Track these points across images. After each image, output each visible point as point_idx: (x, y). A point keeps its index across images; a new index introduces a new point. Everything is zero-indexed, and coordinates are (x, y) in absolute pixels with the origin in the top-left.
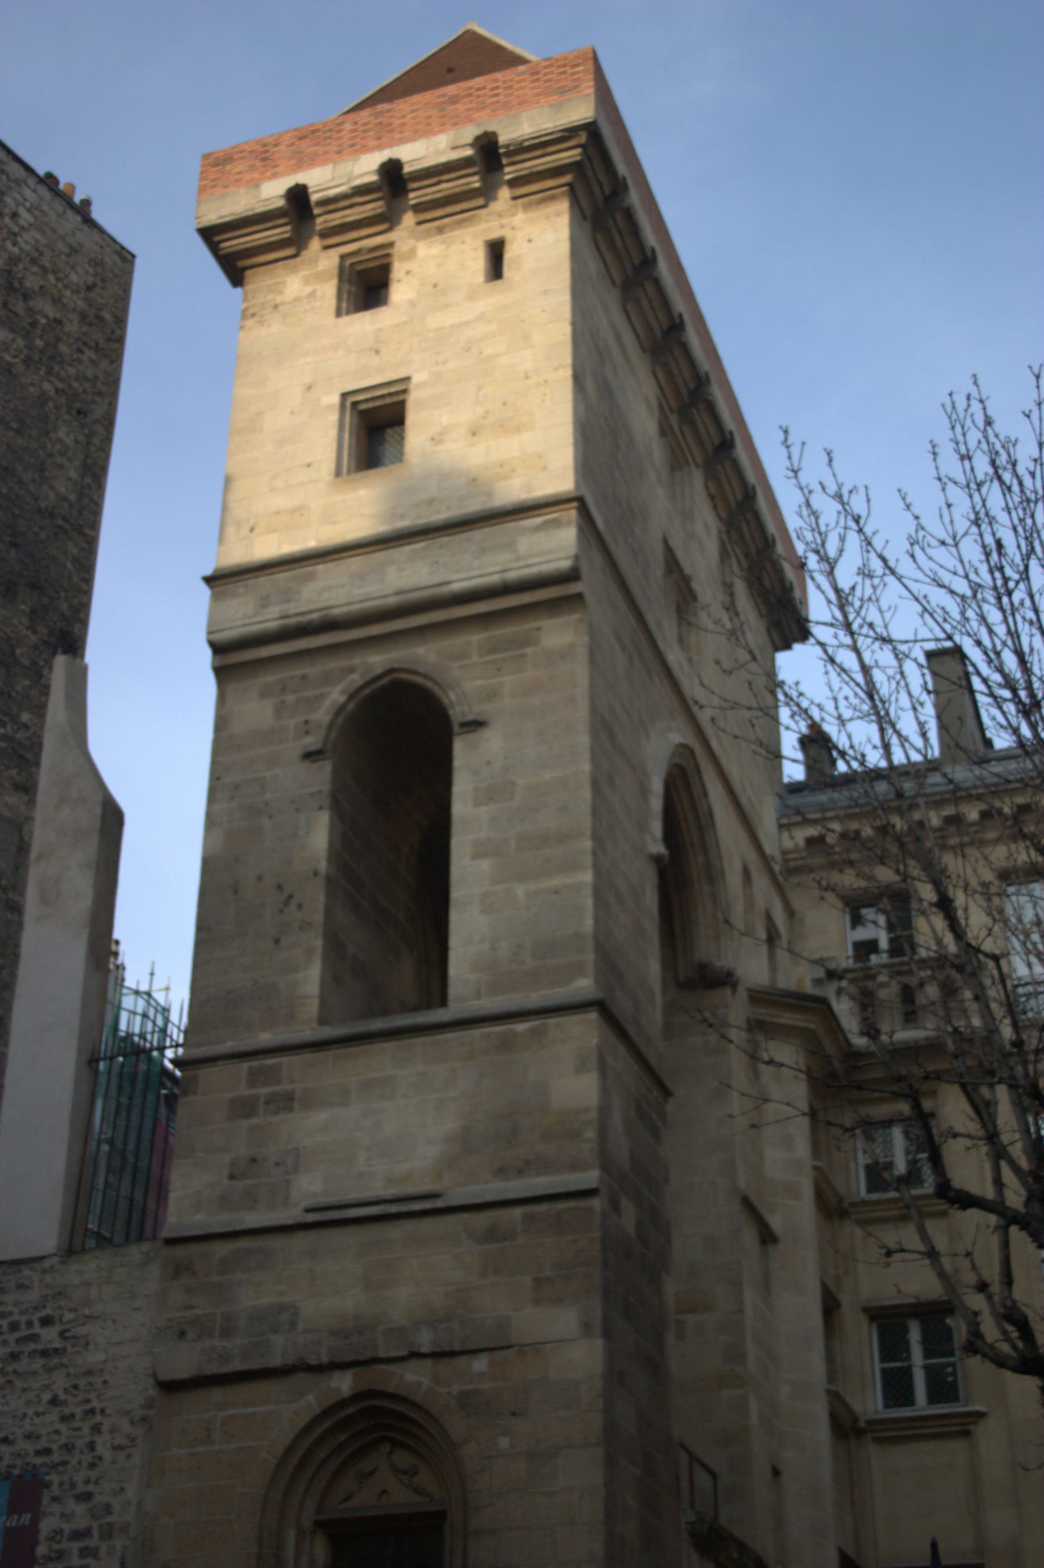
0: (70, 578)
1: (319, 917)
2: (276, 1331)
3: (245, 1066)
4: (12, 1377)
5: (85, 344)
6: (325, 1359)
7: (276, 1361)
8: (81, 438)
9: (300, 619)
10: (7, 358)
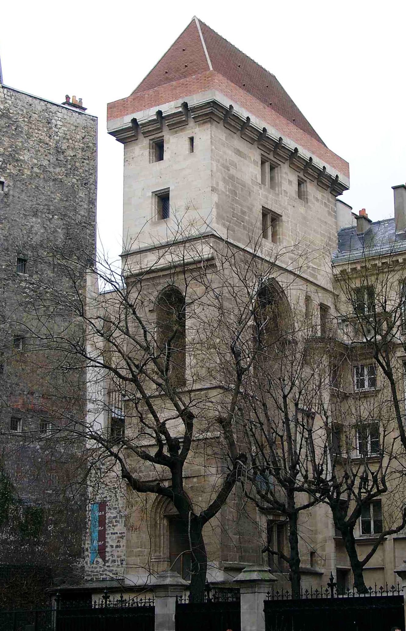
5: (84, 159)
10: (60, 177)
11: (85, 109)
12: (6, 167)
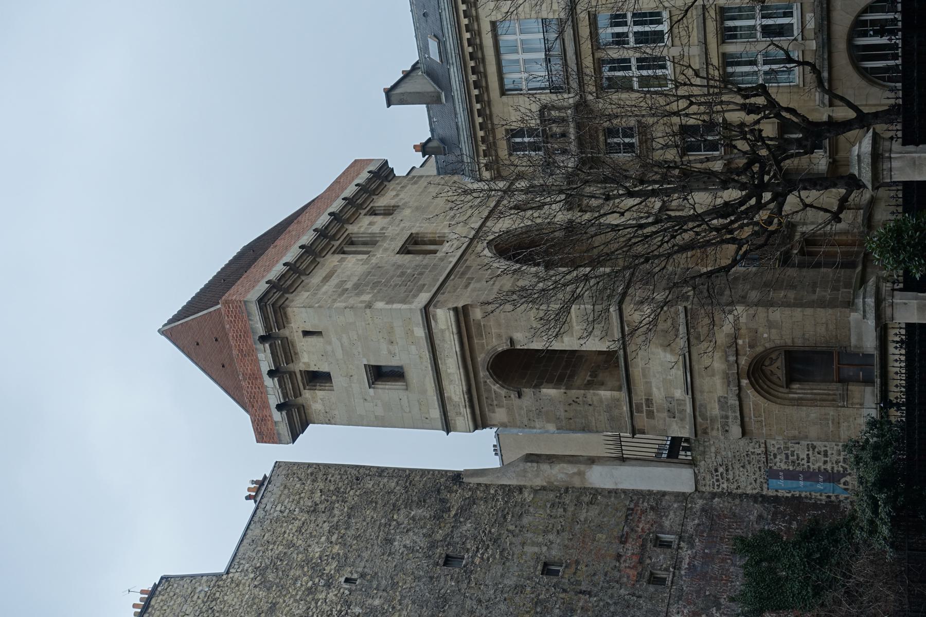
0: (429, 478)
1: (582, 392)
2: (727, 403)
3: (635, 414)
4: (735, 480)
5: (326, 479)
6: (737, 388)
7: (737, 403)
8: (369, 478)
9: (467, 401)
10: (346, 509)
11: (265, 477)
12: (327, 575)
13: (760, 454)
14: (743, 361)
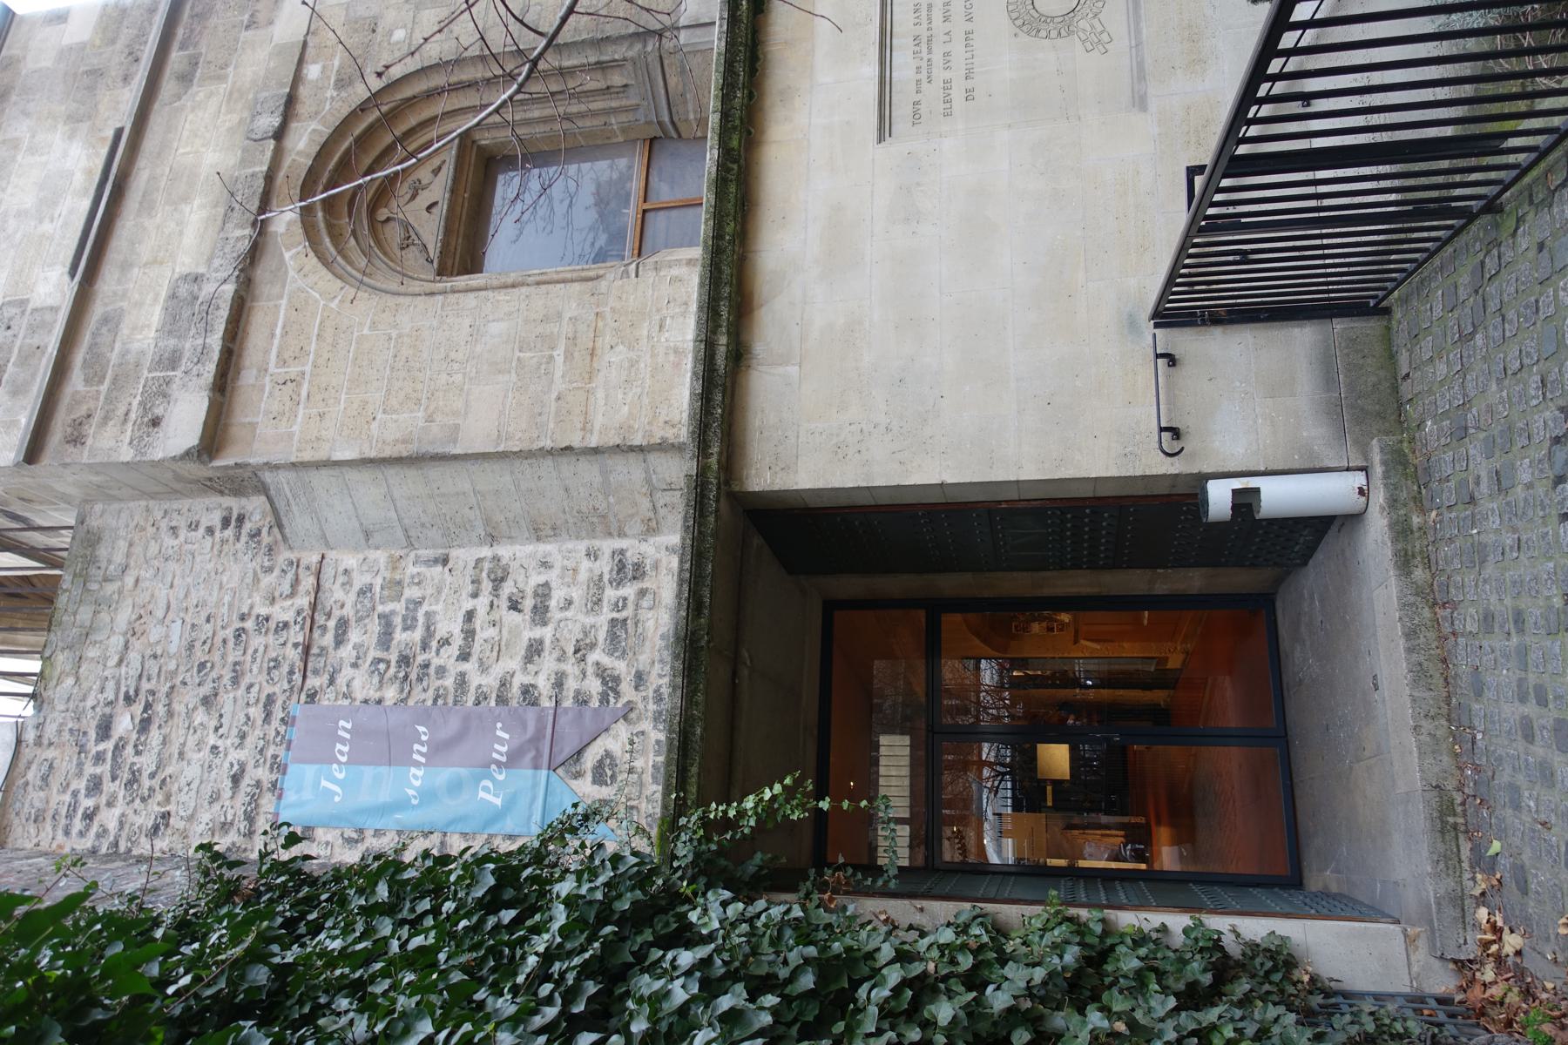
13: (286, 625)
14: (304, 142)
